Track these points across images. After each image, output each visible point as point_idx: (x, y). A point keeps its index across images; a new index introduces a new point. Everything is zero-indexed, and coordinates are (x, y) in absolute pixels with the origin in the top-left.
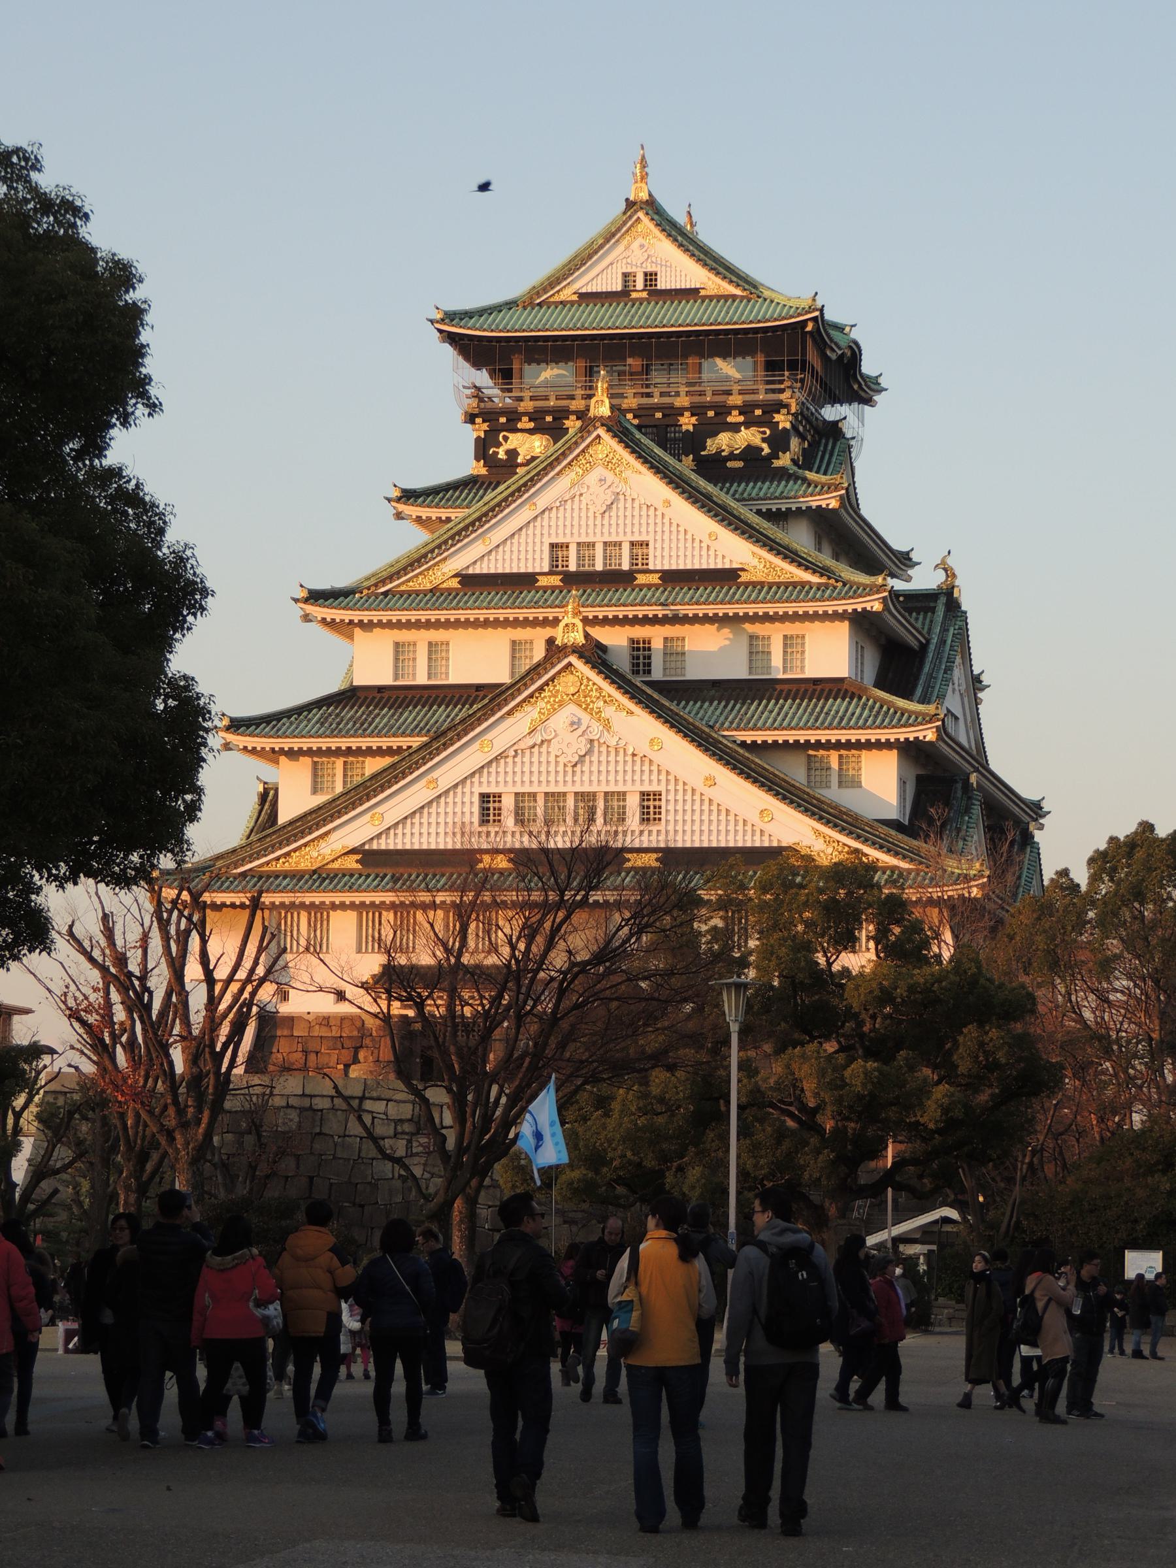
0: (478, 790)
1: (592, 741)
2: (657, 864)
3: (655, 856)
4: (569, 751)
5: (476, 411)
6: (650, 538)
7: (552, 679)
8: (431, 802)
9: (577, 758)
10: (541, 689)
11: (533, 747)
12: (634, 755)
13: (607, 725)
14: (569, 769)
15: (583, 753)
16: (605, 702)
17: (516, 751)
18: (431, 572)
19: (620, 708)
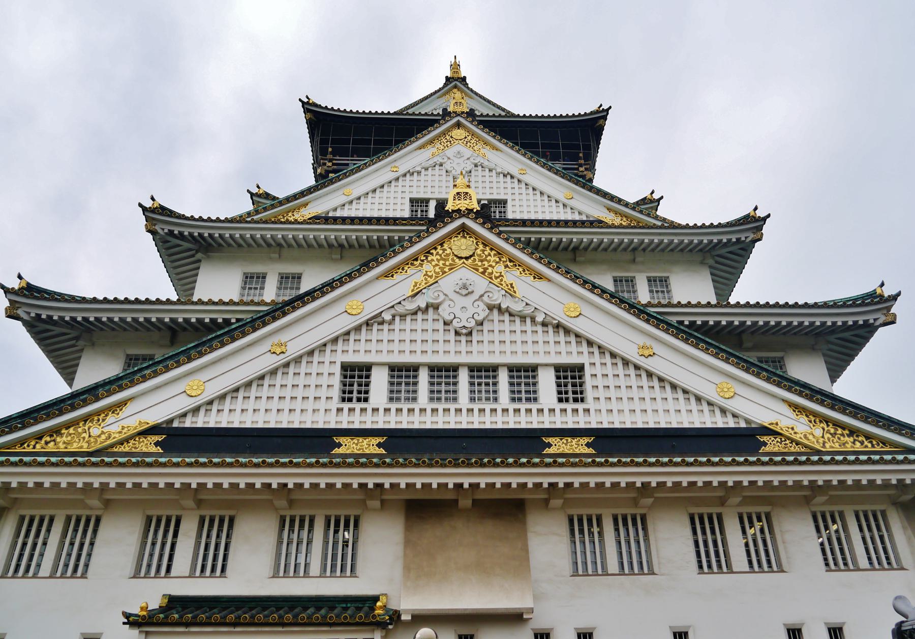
0: (340, 358)
1: (491, 308)
2: (591, 451)
3: (586, 440)
4: (464, 316)
5: (330, 169)
6: (509, 198)
7: (441, 242)
8: (273, 372)
9: (472, 323)
10: (427, 252)
11: (415, 313)
12: (544, 324)
13: (510, 292)
14: (463, 339)
15: (480, 318)
16: (506, 266)
17: (394, 316)
18: (290, 214)
19: (527, 269)
